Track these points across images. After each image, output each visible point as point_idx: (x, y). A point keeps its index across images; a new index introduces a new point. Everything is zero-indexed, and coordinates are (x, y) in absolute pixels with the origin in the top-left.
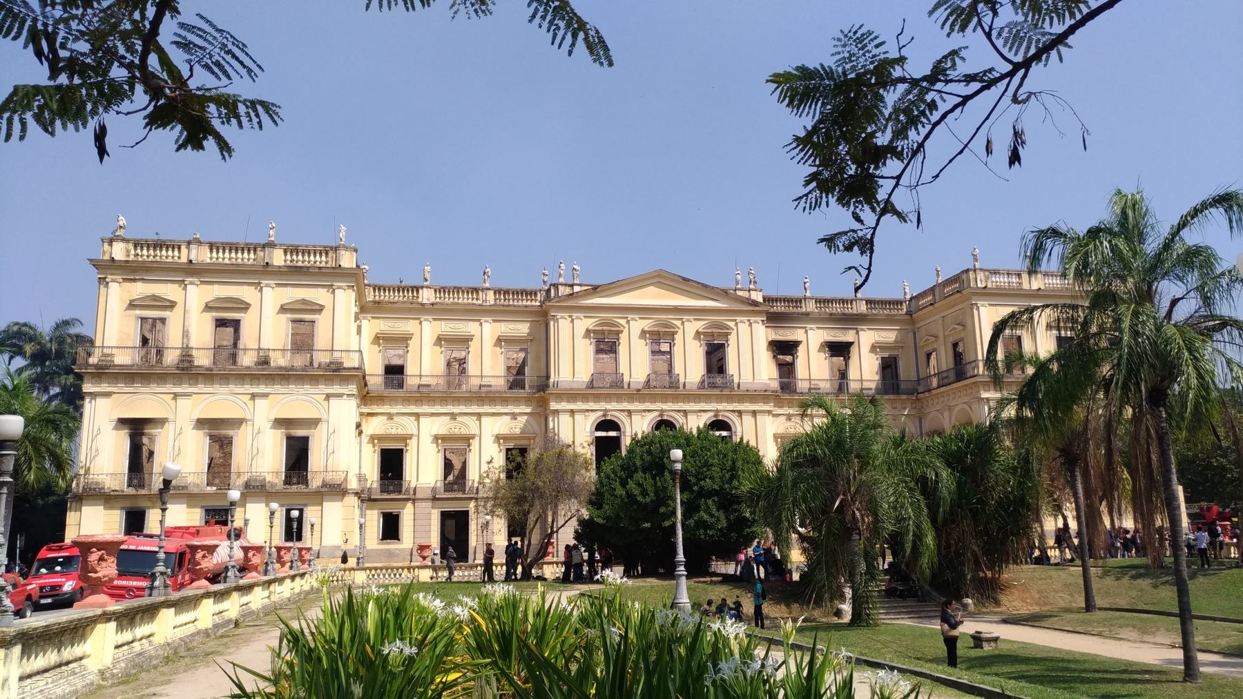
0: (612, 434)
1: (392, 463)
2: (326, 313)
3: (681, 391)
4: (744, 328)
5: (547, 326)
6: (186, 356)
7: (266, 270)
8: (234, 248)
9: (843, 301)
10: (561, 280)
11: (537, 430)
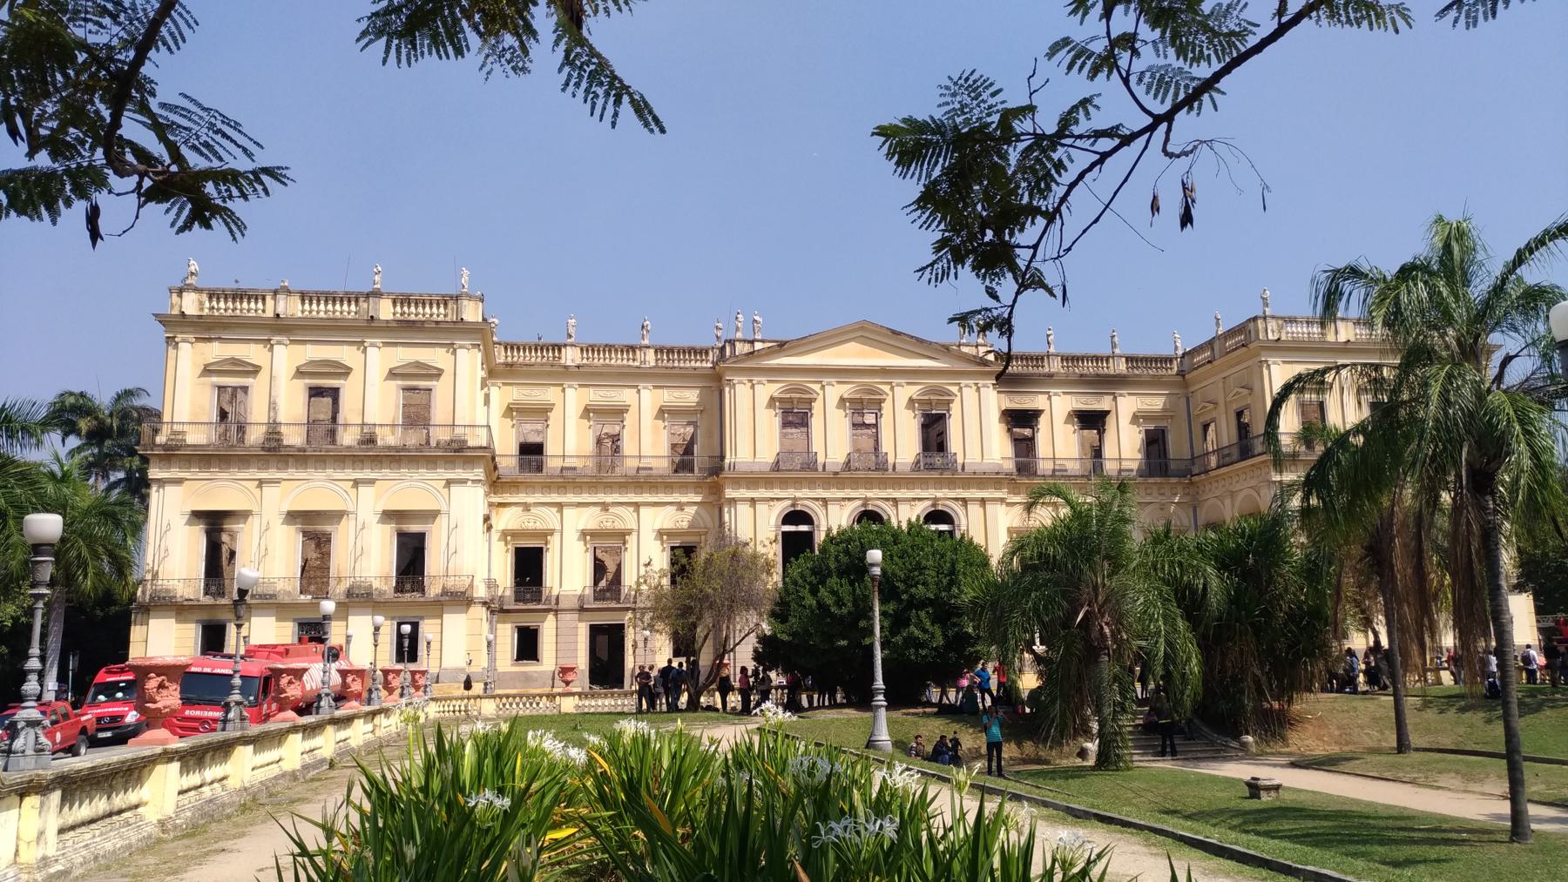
0: (804, 528)
1: (529, 565)
2: (446, 379)
3: (890, 474)
4: (969, 394)
5: (721, 393)
6: (273, 433)
7: (371, 325)
8: (331, 298)
9: (1097, 359)
10: (739, 335)
11: (710, 524)
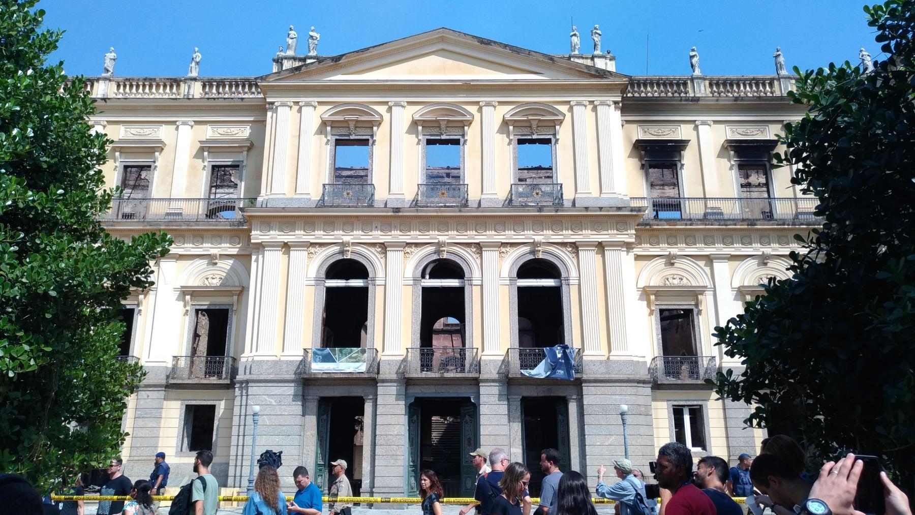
9: (757, 82)
